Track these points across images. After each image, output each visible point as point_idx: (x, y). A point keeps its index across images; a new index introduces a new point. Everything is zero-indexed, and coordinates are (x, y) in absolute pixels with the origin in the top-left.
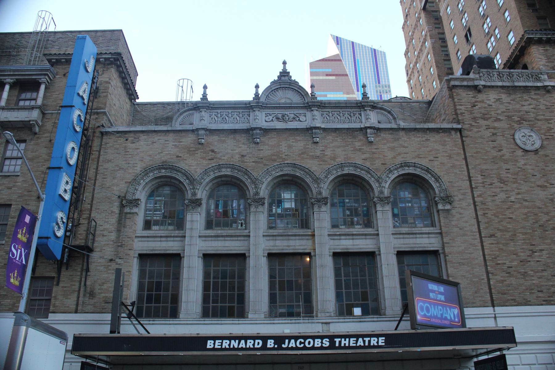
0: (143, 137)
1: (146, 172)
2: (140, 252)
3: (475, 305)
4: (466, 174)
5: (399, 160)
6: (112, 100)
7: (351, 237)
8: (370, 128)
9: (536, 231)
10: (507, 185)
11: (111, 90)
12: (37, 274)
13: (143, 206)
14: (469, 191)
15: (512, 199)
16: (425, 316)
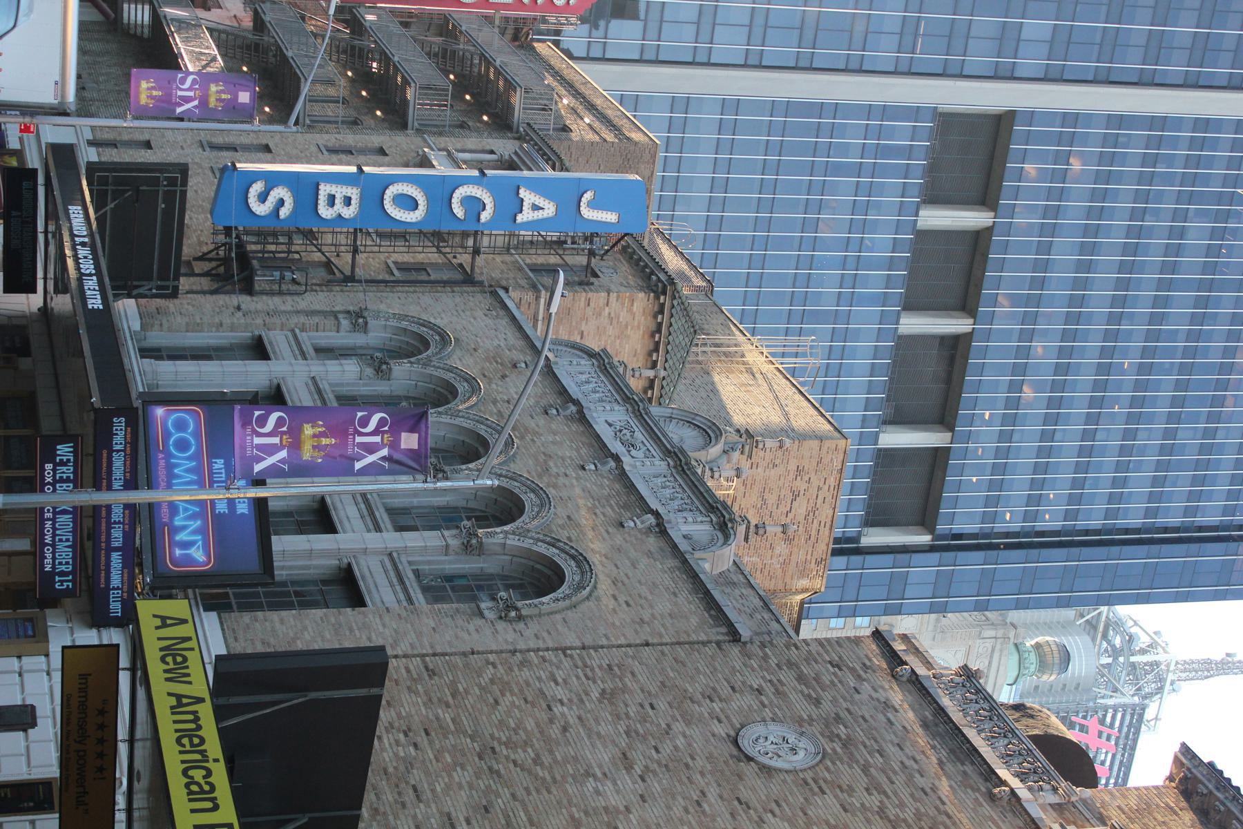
0: (504, 322)
1: (426, 324)
2: (265, 339)
3: (231, 640)
4: (604, 642)
5: (595, 559)
6: (584, 318)
7: (366, 513)
8: (657, 514)
9: (472, 738)
10: (600, 702)
11: (599, 298)
12: (194, 263)
13: (359, 339)
14: (551, 645)
15: (558, 709)
16: (167, 435)
